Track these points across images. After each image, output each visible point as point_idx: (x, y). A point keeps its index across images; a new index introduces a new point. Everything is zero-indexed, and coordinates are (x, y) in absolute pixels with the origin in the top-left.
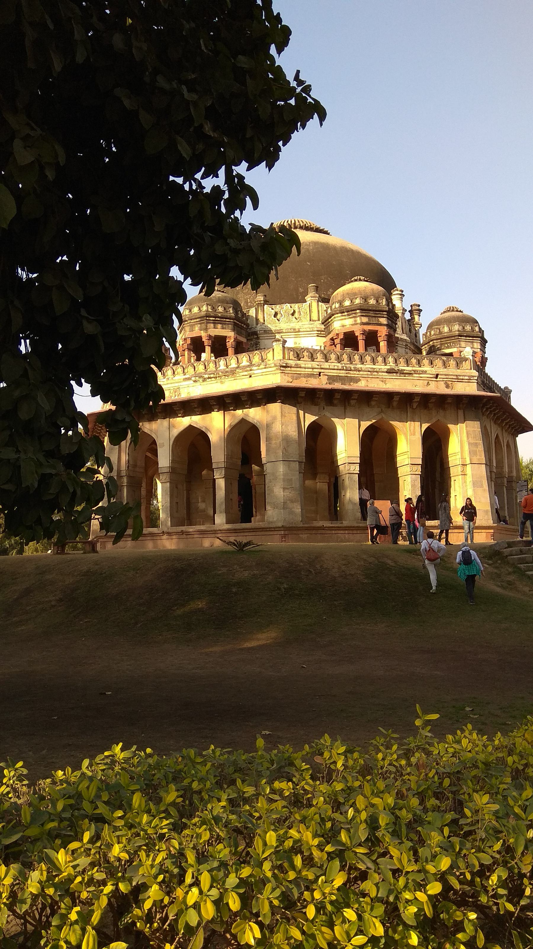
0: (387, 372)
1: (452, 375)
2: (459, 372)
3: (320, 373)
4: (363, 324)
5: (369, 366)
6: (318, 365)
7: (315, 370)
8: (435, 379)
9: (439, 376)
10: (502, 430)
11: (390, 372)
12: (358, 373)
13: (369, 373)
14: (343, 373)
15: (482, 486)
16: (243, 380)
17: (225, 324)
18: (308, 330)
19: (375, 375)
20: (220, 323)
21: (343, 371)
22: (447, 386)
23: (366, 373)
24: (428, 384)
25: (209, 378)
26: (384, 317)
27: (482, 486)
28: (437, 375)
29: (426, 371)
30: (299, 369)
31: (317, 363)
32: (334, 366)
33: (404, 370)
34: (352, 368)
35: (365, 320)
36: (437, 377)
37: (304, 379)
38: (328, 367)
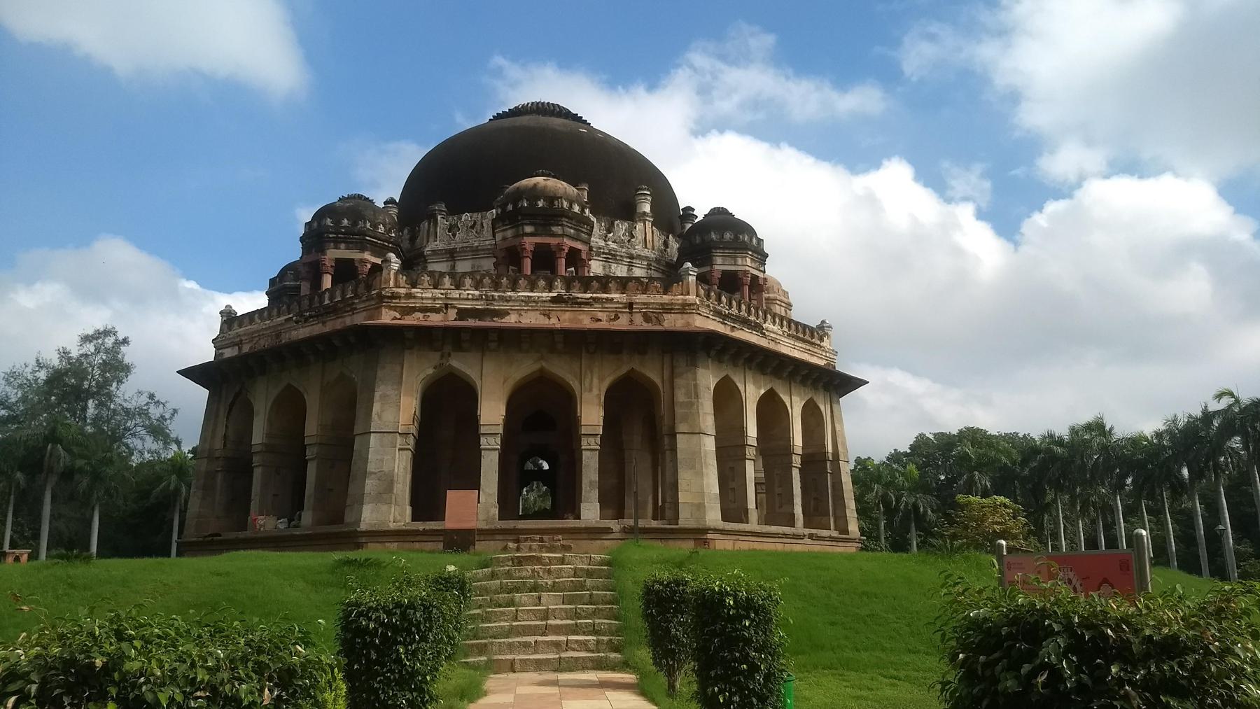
2: (666, 299)
6: (442, 294)
10: (790, 384)
12: (506, 304)
14: (480, 305)
15: (693, 467)
17: (352, 243)
19: (532, 306)
22: (647, 318)
24: (617, 318)
25: (311, 316)
26: (560, 225)
27: (693, 467)
29: (612, 299)
30: (413, 301)
31: (442, 291)
32: (468, 294)
33: (578, 298)
34: (496, 298)
35: (528, 229)
37: (420, 315)
38: (458, 296)
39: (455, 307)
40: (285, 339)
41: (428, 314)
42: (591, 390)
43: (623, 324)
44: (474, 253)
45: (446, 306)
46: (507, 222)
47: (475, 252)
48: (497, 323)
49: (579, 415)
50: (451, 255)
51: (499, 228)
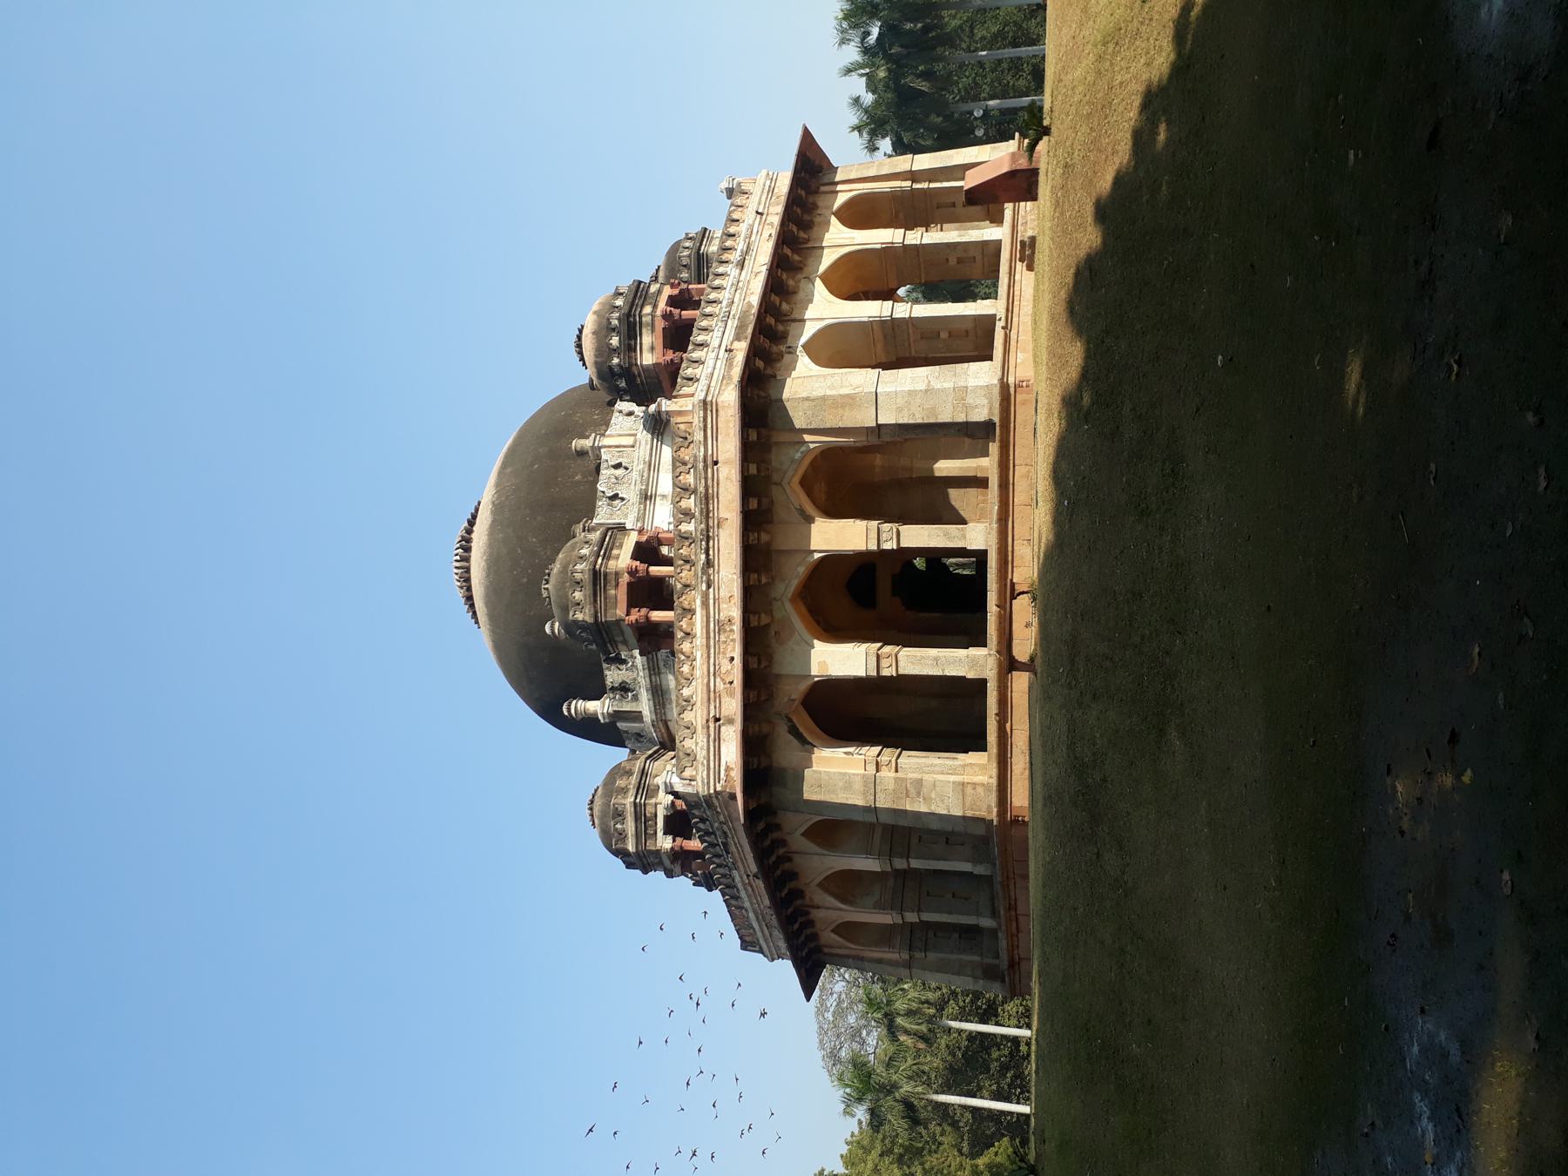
0: (742, 270)
1: (761, 198)
3: (726, 351)
4: (653, 315)
5: (725, 296)
7: (721, 356)
8: (764, 216)
9: (760, 211)
11: (741, 264)
12: (735, 305)
13: (738, 291)
16: (721, 478)
18: (649, 447)
20: (612, 549)
21: (730, 322)
23: (737, 295)
28: (757, 212)
34: (727, 310)
35: (648, 309)
36: (761, 214)
39: (732, 343)
40: (732, 610)
41: (735, 363)
42: (853, 238)
43: (775, 220)
44: (652, 468)
45: (729, 351)
46: (633, 343)
47: (652, 466)
48: (754, 311)
49: (878, 246)
50: (647, 497)
51: (636, 359)
